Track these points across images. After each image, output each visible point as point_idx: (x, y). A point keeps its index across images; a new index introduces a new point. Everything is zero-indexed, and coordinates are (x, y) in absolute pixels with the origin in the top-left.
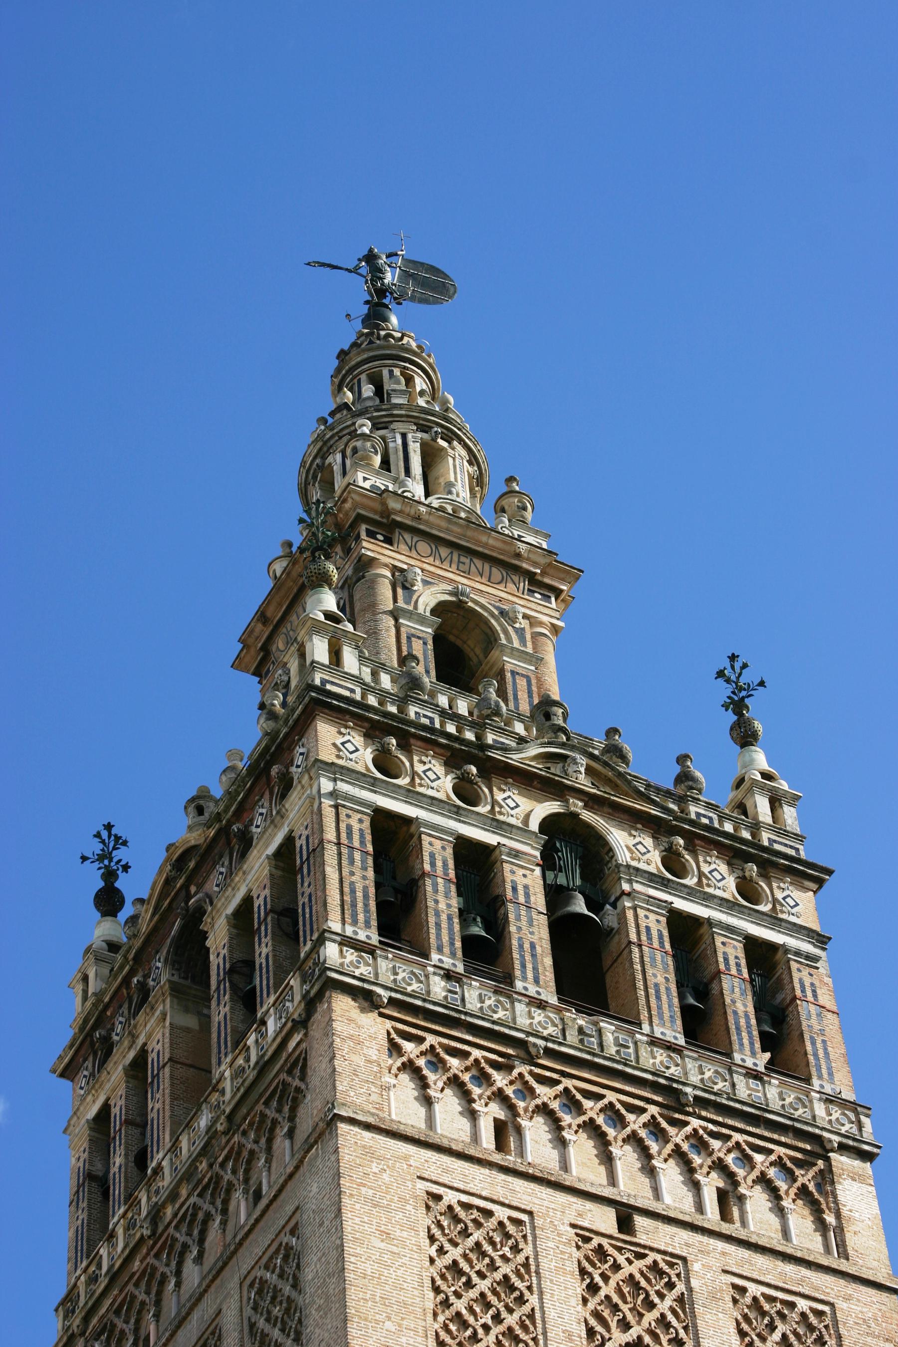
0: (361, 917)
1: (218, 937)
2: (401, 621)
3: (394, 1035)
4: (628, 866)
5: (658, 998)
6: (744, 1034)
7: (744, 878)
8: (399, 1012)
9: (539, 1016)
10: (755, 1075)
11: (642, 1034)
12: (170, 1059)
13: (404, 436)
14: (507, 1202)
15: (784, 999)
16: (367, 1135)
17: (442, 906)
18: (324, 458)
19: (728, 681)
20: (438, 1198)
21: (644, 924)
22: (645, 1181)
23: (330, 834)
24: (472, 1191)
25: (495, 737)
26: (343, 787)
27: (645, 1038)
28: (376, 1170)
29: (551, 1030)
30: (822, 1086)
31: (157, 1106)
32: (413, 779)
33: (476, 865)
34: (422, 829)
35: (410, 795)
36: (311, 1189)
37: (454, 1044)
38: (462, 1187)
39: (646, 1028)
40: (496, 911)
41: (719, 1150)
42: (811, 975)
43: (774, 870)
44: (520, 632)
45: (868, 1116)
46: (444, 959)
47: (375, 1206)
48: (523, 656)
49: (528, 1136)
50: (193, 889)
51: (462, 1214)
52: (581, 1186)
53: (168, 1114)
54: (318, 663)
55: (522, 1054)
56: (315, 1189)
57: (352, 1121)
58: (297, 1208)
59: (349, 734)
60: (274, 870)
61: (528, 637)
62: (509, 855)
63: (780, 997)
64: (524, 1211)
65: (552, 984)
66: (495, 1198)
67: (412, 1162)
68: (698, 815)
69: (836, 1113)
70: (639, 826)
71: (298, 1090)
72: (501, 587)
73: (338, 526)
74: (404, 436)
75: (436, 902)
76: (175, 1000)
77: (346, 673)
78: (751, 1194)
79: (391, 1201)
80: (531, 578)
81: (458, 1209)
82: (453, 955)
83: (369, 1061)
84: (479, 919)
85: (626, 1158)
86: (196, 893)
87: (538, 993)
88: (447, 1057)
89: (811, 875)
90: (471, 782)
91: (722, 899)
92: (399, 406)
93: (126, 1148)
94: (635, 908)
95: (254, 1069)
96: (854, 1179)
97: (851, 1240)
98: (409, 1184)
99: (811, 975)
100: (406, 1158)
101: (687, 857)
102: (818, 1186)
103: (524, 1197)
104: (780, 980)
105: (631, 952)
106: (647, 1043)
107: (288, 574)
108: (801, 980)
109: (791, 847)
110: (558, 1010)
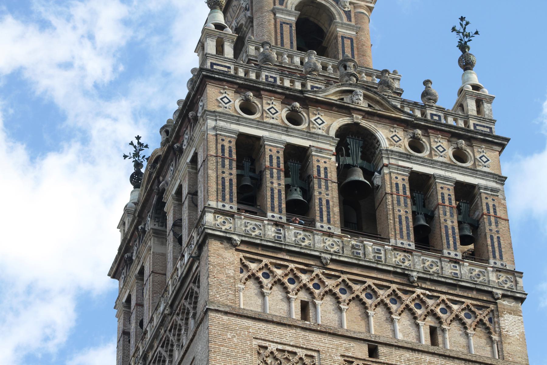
0: (227, 197)
2: (277, 15)
3: (244, 261)
4: (387, 150)
5: (400, 223)
6: (451, 239)
7: (458, 148)
8: (248, 248)
9: (329, 241)
10: (456, 261)
11: (389, 245)
12: (152, 272)
14: (305, 347)
15: (479, 215)
16: (225, 318)
17: (275, 185)
19: (458, 32)
20: (266, 348)
22: (388, 326)
23: (212, 152)
24: (284, 342)
25: (312, 84)
26: (221, 124)
28: (229, 336)
29: (336, 248)
30: (495, 263)
32: (263, 113)
34: (266, 143)
35: (260, 124)
36: (198, 348)
37: (279, 262)
38: (279, 341)
39: (393, 242)
40: (309, 184)
41: (432, 306)
42: (493, 200)
43: (475, 142)
44: (348, 14)
45: (521, 277)
46: (275, 215)
47: (228, 356)
48: (349, 27)
49: (320, 309)
50: (161, 178)
51: (279, 355)
52: (348, 334)
54: (209, 54)
55: (318, 263)
56: (200, 348)
57: (217, 311)
58: (194, 358)
59: (225, 93)
60: (191, 170)
61: (352, 15)
62: (316, 151)
63: (477, 213)
64: (315, 351)
65: (338, 222)
66: (298, 345)
67: (251, 330)
68: (432, 115)
69: (503, 277)
70: (395, 126)
71: (196, 292)
75: (272, 183)
76: (156, 239)
77: (225, 58)
78: (449, 328)
79: (238, 352)
81: (276, 353)
82: (280, 212)
83: (229, 277)
84: (298, 189)
85: (377, 315)
86: (163, 180)
87: (329, 228)
88: (275, 270)
90: (297, 112)
91: (442, 162)
95: (179, 281)
96: (510, 313)
97: (507, 348)
98: (248, 342)
99: (493, 200)
100: (248, 328)
101: (424, 140)
102: (490, 320)
103: (315, 343)
104: (477, 204)
106: (392, 250)
108: (487, 204)
109: (487, 127)
110: (340, 237)
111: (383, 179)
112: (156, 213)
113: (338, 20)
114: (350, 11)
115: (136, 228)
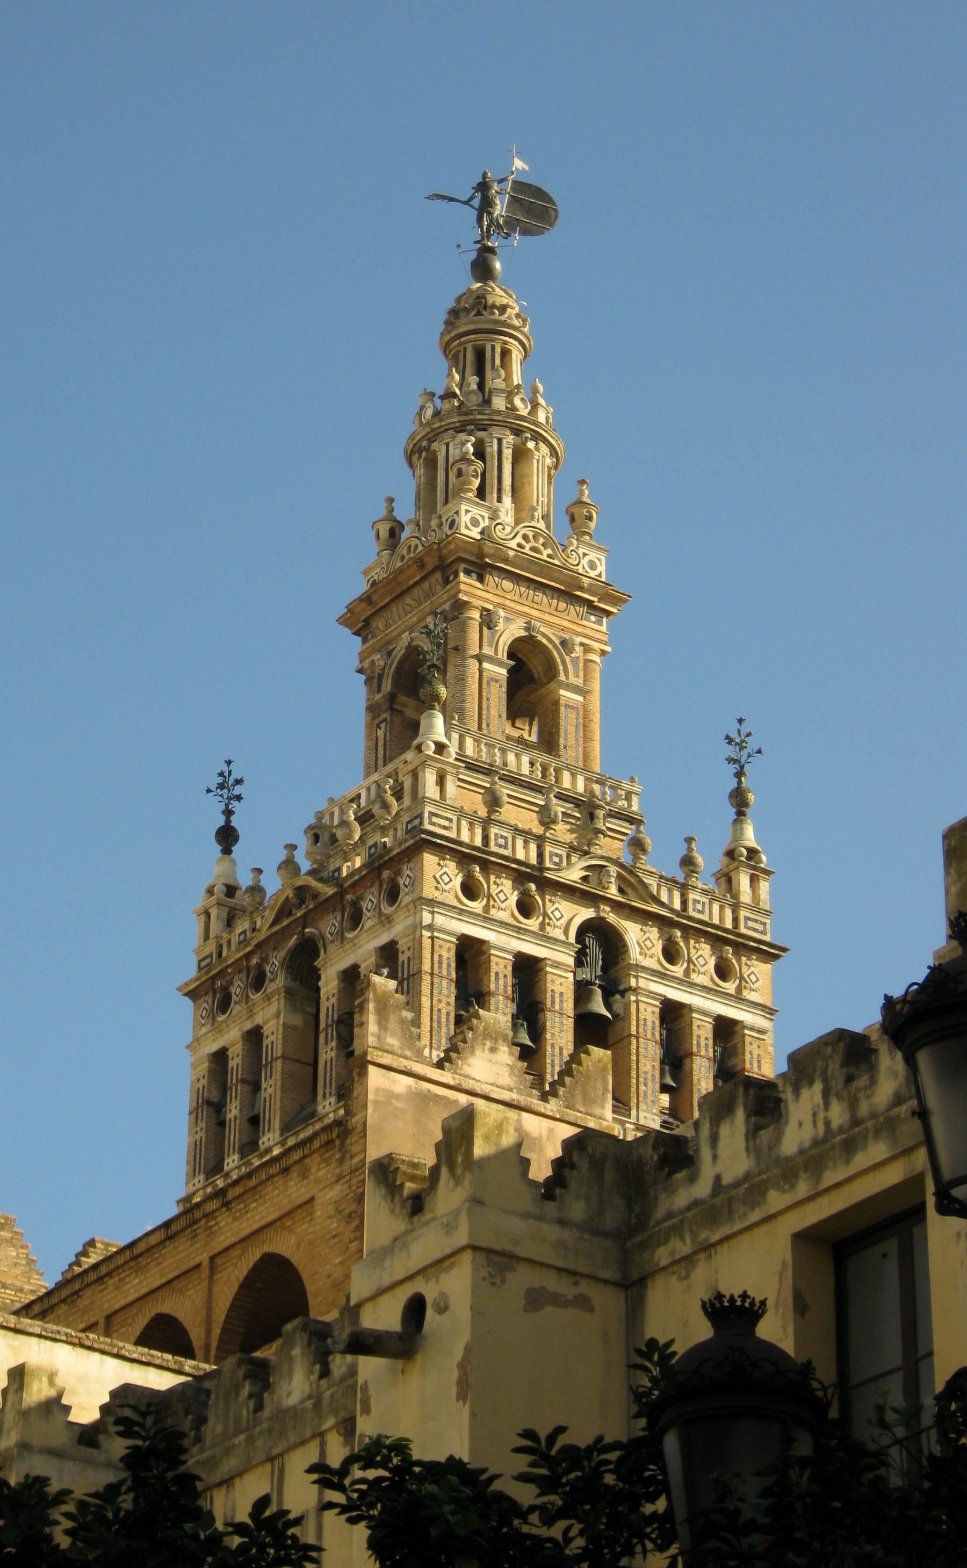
1: (329, 984)
4: (637, 965)
7: (722, 957)
11: (630, 1123)
12: (283, 1057)
13: (500, 441)
18: (431, 441)
21: (644, 1016)
23: (426, 967)
27: (632, 1127)
31: (270, 1091)
33: (527, 970)
44: (575, 661)
53: (278, 1104)
62: (552, 966)
72: (564, 615)
73: (441, 559)
74: (500, 441)
80: (590, 604)
89: (770, 953)
92: (499, 412)
93: (241, 1104)
94: (637, 1002)
99: (759, 1047)
104: (735, 1047)
105: (630, 1044)
106: (633, 1130)
107: (395, 578)
109: (761, 923)
111: (627, 1006)
112: (290, 961)
113: (562, 677)
114: (578, 658)
115: (248, 956)
